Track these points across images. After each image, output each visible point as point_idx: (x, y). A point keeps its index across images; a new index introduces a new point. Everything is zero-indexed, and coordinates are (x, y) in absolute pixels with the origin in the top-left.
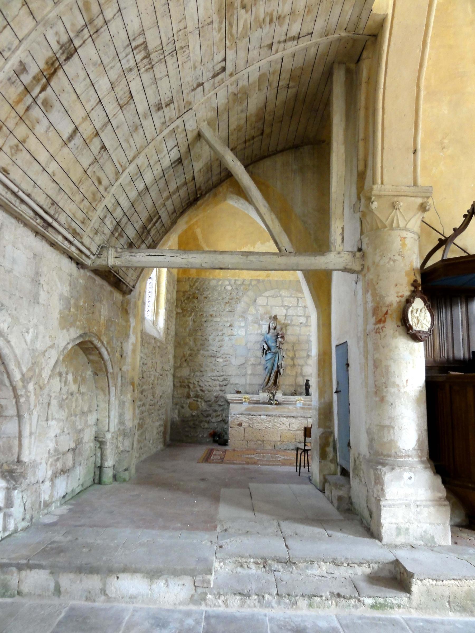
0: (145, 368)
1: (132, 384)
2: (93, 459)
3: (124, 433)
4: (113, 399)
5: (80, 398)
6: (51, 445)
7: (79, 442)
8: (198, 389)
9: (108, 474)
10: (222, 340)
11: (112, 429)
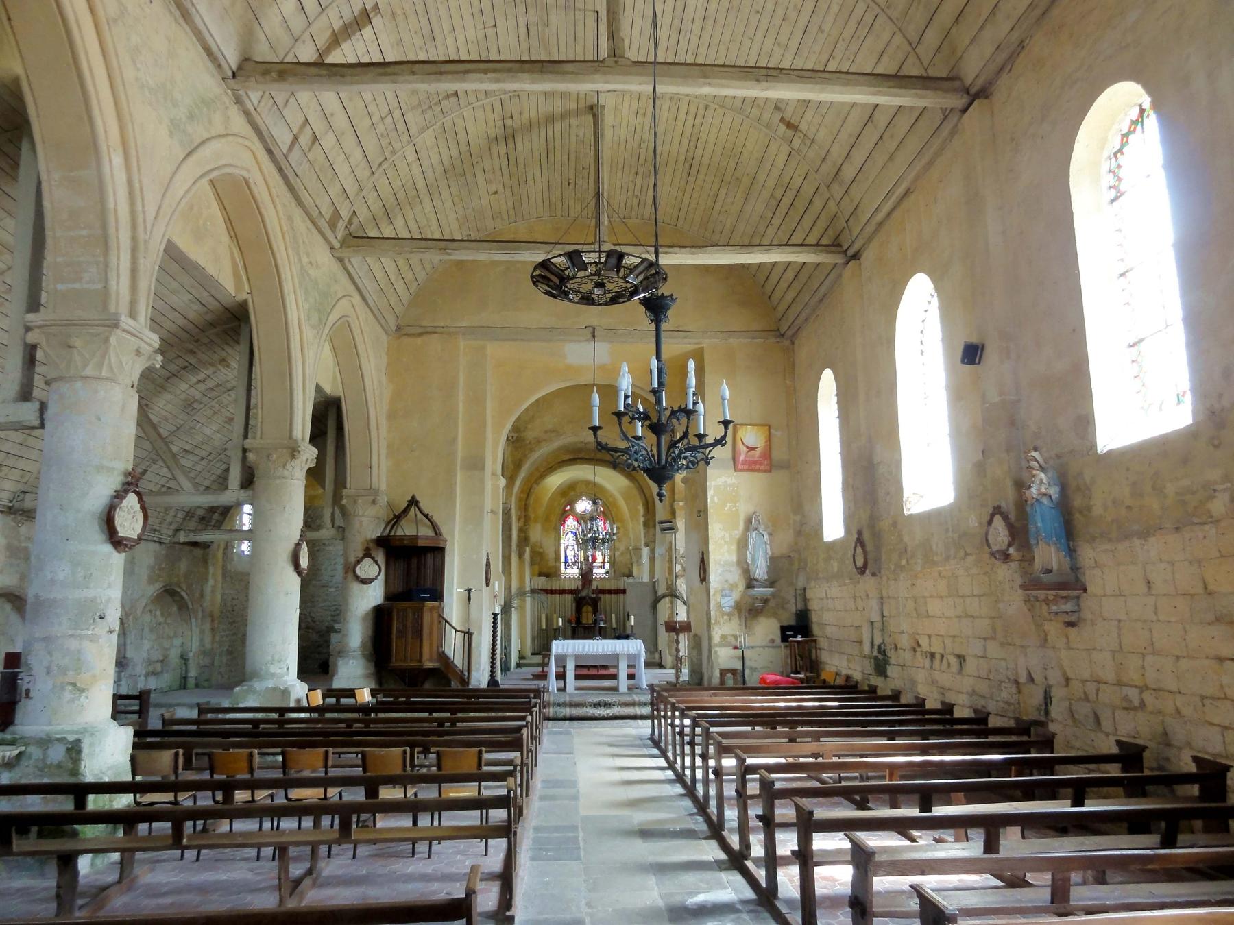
0: (235, 602)
1: (212, 616)
2: (179, 671)
3: (204, 653)
4: (194, 628)
5: (166, 627)
6: (145, 655)
7: (166, 657)
8: (310, 620)
9: (191, 682)
10: (335, 570)
11: (194, 650)
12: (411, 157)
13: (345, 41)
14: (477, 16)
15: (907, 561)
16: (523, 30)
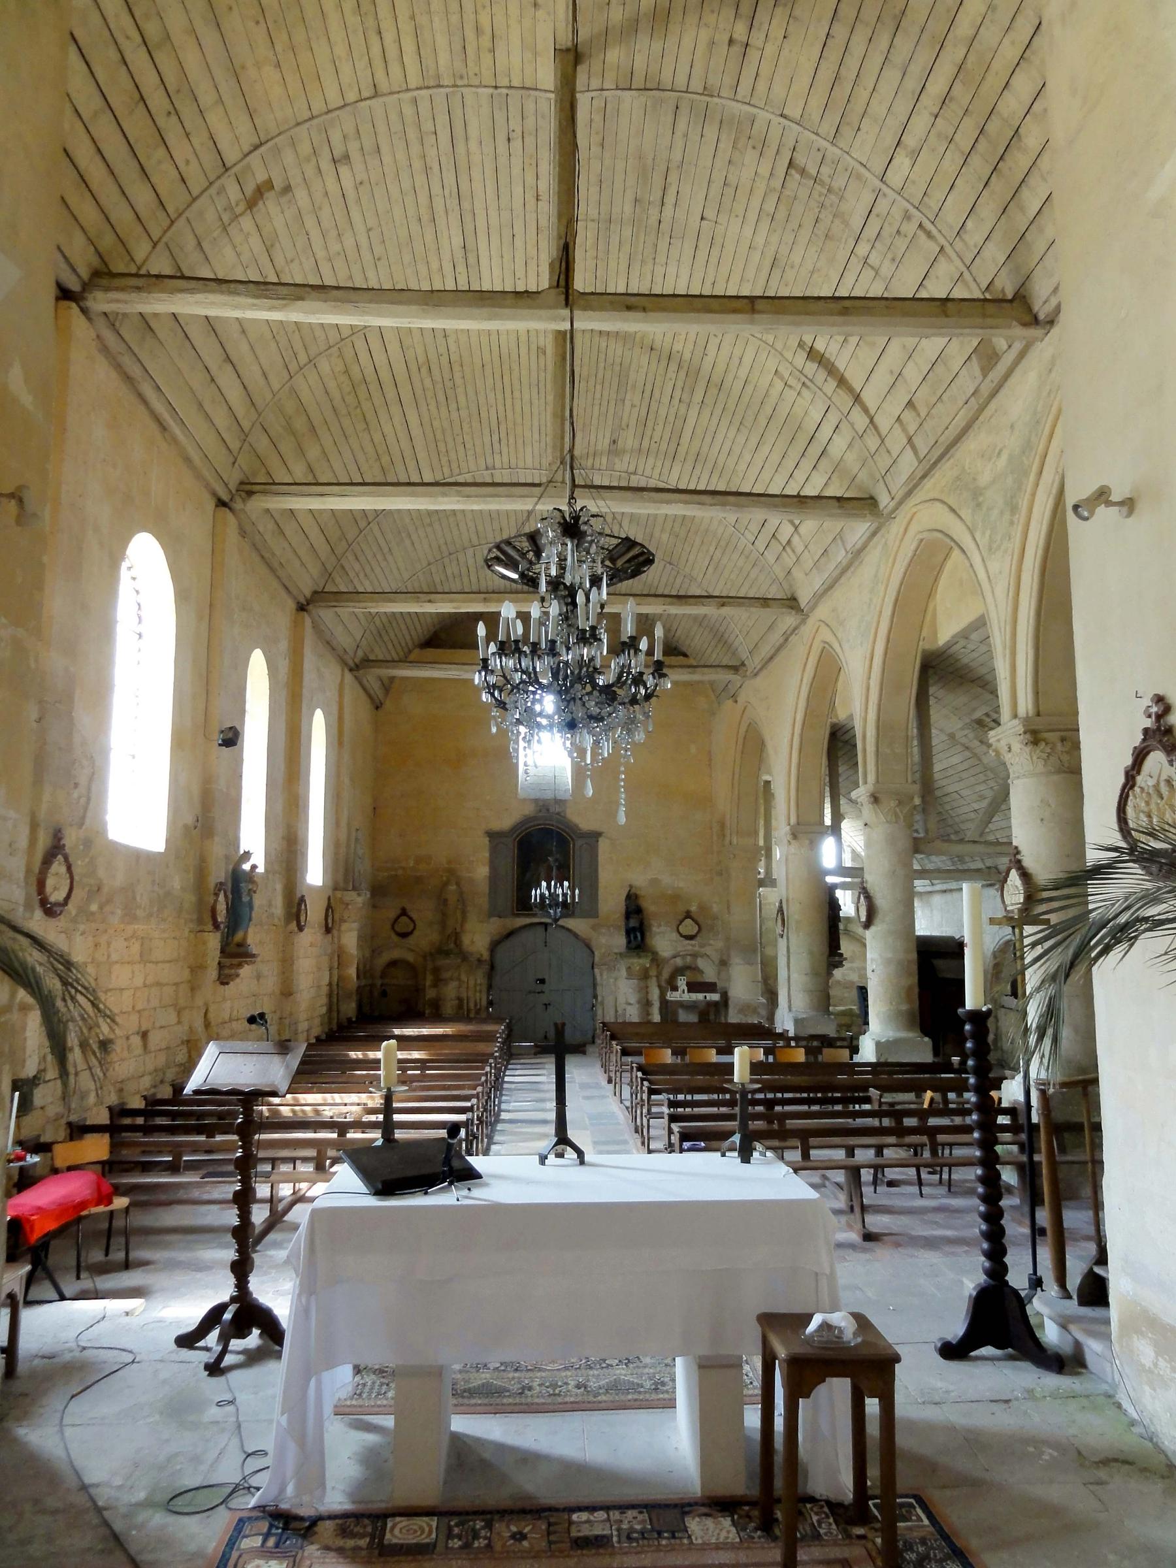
12: (902, 162)
13: (838, 370)
14: (718, 241)
15: (101, 908)
16: (670, 199)
